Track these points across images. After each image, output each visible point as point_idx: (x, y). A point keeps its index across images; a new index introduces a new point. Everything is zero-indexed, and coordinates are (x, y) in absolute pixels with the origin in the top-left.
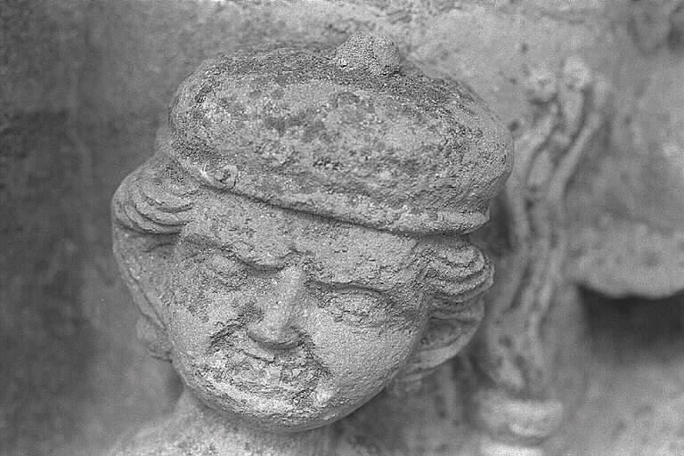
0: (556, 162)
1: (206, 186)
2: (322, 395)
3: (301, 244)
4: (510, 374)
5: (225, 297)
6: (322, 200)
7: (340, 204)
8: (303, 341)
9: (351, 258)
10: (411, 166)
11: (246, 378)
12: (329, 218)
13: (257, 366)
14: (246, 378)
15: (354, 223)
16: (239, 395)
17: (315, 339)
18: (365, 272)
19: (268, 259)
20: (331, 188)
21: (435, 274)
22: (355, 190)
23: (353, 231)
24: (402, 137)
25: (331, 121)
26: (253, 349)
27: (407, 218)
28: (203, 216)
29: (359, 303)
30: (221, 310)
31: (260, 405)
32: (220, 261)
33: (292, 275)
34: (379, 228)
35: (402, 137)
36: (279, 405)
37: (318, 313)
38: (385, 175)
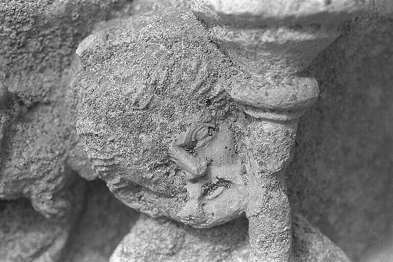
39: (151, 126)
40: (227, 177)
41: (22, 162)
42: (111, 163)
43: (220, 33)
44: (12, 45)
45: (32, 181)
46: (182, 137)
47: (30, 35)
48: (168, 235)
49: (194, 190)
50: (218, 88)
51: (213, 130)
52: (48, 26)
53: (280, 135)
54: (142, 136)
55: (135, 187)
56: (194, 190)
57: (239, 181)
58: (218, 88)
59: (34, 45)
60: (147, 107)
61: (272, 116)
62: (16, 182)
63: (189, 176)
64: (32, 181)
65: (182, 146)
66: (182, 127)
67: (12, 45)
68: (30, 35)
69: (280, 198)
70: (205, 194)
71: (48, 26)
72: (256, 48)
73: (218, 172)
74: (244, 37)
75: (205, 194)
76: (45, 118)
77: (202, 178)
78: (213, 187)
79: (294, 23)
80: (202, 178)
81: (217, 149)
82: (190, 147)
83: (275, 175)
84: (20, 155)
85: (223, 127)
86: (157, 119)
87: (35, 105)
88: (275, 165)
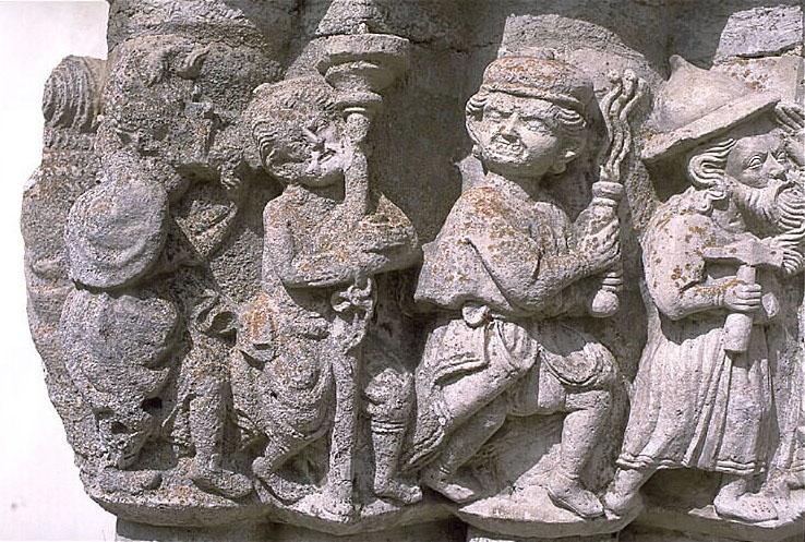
0: (622, 106)
1: (491, 91)
2: (525, 155)
3: (517, 105)
4: (603, 174)
5: (496, 125)
6: (522, 90)
7: (528, 91)
8: (518, 137)
9: (532, 108)
10: (549, 78)
11: (501, 150)
12: (524, 96)
13: (505, 146)
14: (501, 150)
15: (532, 97)
16: (498, 156)
17: (522, 136)
18: (536, 113)
19: (508, 111)
20: (525, 86)
21: (560, 116)
22: (532, 86)
23: (533, 100)
24: (547, 70)
25: (525, 66)
26: (503, 140)
27: (548, 95)
28: (491, 100)
29: (536, 123)
30: (495, 128)
31: (506, 159)
32: (494, 114)
33: (515, 115)
34: (540, 98)
35: (547, 70)
36: (511, 158)
37: (522, 128)
38: (541, 81)
39: (294, 117)
40: (334, 149)
41: (219, 148)
42: (271, 138)
43: (331, 70)
44: (217, 91)
45: (223, 161)
46: (310, 123)
47: (227, 86)
48: (299, 191)
49: (315, 155)
50: (329, 101)
51: (327, 124)
52: (238, 82)
53: (362, 121)
54: (289, 122)
55: (282, 159)
56: (315, 155)
57: (340, 151)
58: (329, 101)
59: (228, 93)
60: (292, 107)
61: (355, 109)
62: (215, 160)
63: (313, 145)
64: (223, 161)
65: (309, 128)
66: (310, 118)
67: (217, 91)
68: (227, 86)
69: (361, 157)
70: (321, 158)
71: (238, 82)
72: (349, 73)
73: (327, 145)
74: (343, 67)
75: (321, 158)
76: (230, 131)
77: (320, 147)
78: (325, 155)
79: (367, 57)
80: (320, 147)
81: (328, 133)
82: (313, 130)
83: (358, 144)
84: (218, 144)
85: (332, 123)
86: (297, 113)
87: (228, 123)
88: (358, 138)
